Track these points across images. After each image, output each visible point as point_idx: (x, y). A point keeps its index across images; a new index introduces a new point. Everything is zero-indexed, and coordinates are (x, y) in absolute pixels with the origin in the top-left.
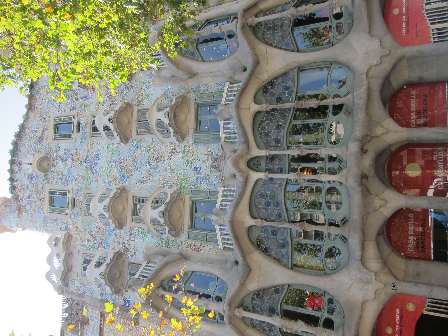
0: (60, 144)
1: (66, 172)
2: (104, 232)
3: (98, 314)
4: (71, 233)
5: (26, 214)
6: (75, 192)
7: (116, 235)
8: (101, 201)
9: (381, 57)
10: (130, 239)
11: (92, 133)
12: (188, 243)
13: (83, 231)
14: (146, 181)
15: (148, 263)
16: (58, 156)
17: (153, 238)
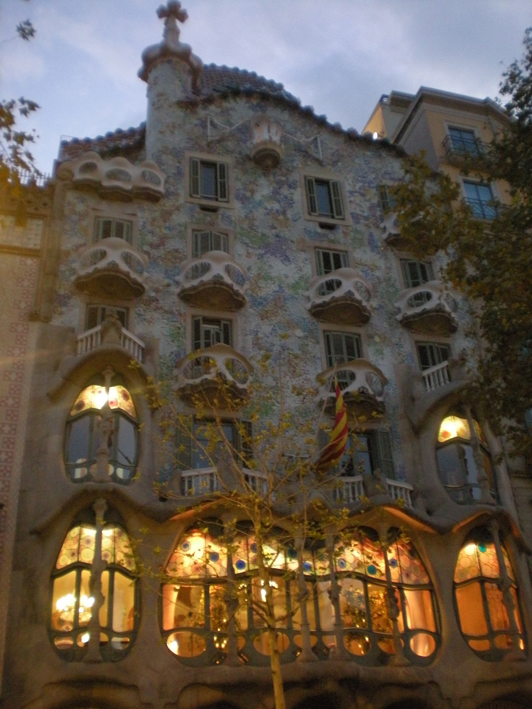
0: (299, 190)
1: (258, 197)
2: (170, 264)
3: (35, 245)
4: (162, 202)
5: (182, 114)
6: (228, 213)
7: (168, 285)
8: (228, 270)
9: (449, 699)
10: (166, 312)
11: (321, 251)
12: (171, 413)
13: (167, 224)
14: (257, 344)
15: (143, 349)
16: (280, 184)
17: (172, 353)
